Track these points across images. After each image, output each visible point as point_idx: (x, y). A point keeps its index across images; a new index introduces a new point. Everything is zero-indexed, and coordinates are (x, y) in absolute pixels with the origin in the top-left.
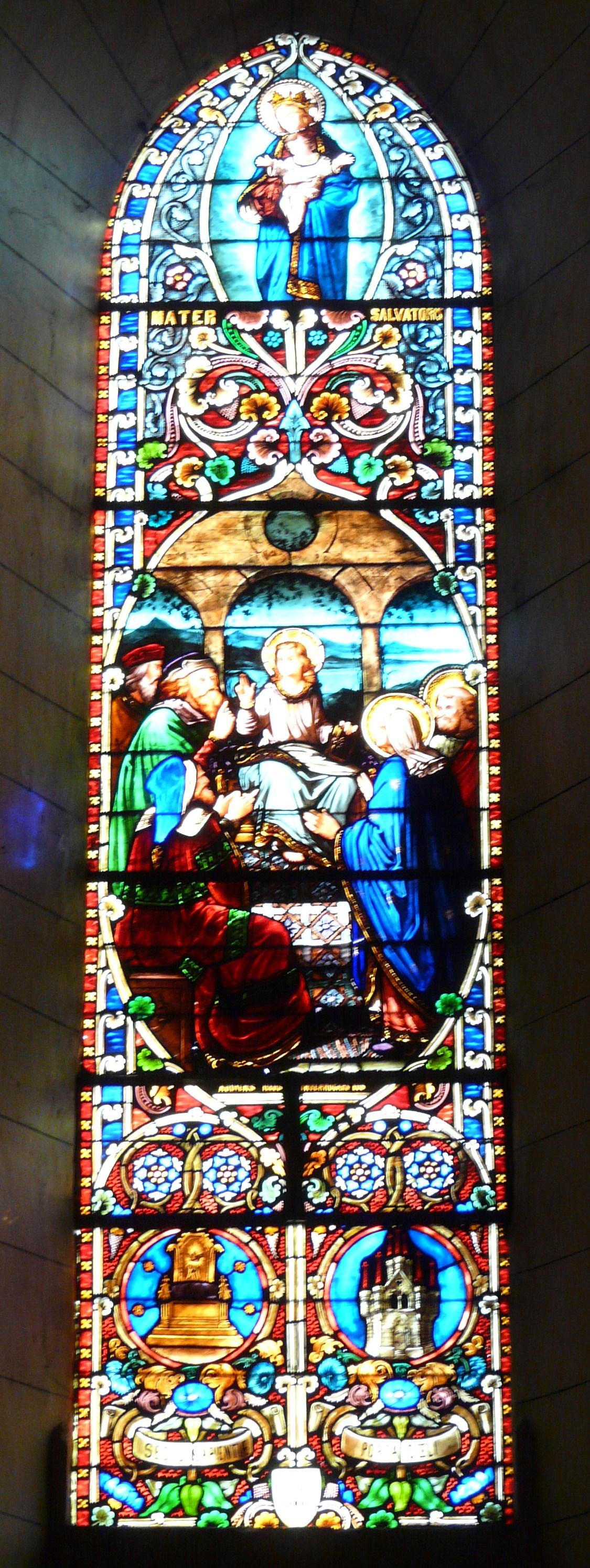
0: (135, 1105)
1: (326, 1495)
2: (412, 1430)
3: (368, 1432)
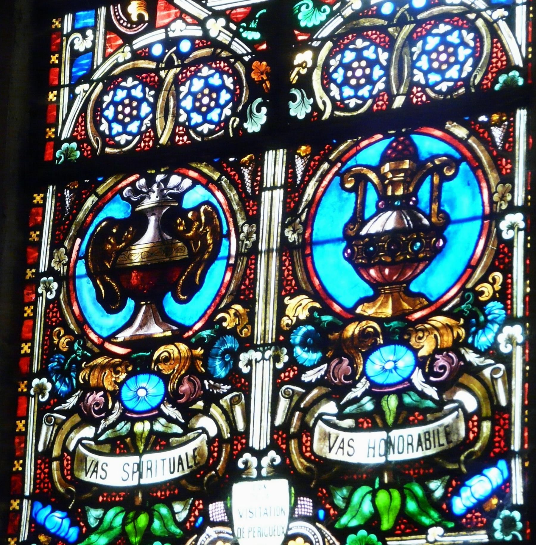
0: (110, 27)
1: (298, 511)
2: (404, 414)
3: (349, 423)
